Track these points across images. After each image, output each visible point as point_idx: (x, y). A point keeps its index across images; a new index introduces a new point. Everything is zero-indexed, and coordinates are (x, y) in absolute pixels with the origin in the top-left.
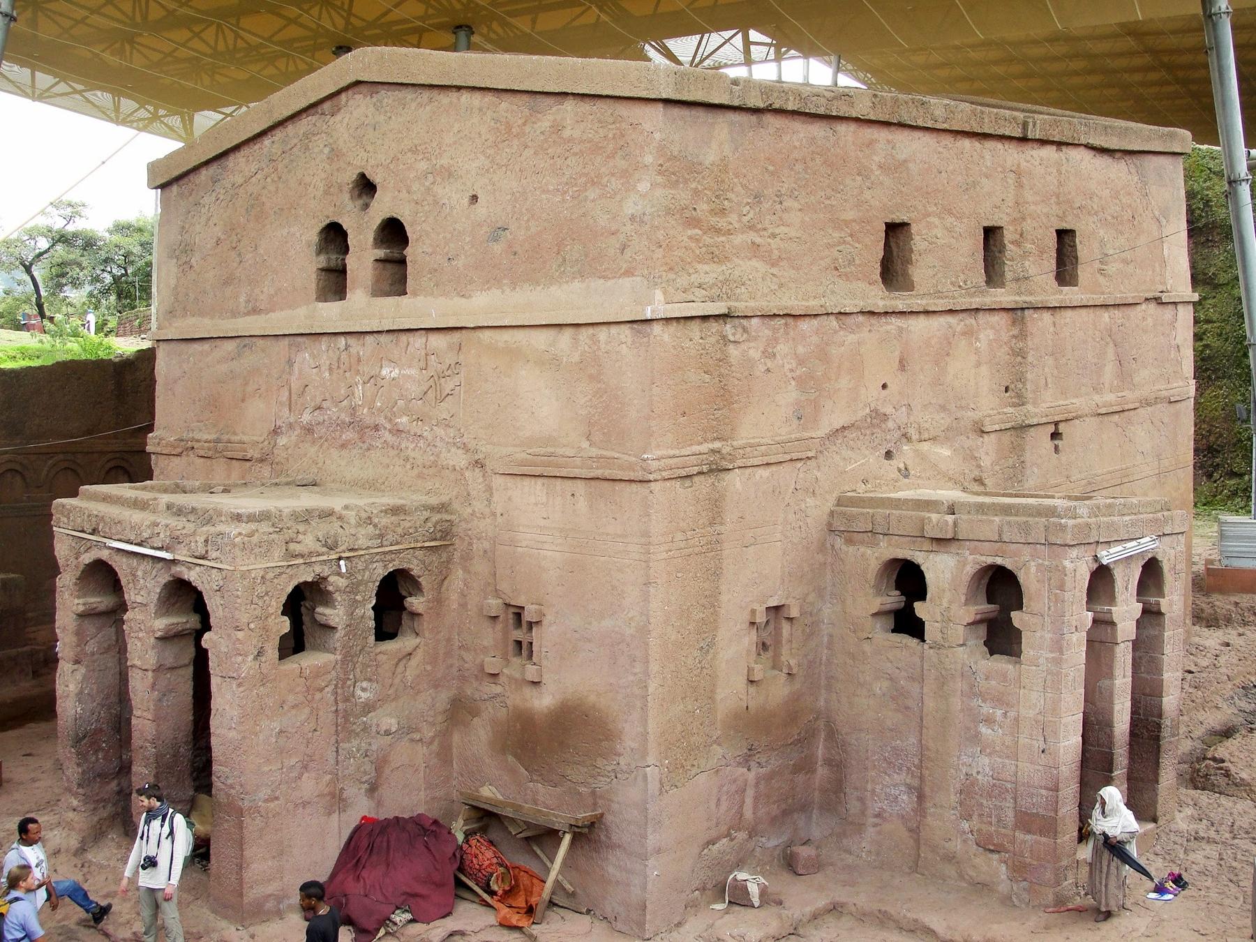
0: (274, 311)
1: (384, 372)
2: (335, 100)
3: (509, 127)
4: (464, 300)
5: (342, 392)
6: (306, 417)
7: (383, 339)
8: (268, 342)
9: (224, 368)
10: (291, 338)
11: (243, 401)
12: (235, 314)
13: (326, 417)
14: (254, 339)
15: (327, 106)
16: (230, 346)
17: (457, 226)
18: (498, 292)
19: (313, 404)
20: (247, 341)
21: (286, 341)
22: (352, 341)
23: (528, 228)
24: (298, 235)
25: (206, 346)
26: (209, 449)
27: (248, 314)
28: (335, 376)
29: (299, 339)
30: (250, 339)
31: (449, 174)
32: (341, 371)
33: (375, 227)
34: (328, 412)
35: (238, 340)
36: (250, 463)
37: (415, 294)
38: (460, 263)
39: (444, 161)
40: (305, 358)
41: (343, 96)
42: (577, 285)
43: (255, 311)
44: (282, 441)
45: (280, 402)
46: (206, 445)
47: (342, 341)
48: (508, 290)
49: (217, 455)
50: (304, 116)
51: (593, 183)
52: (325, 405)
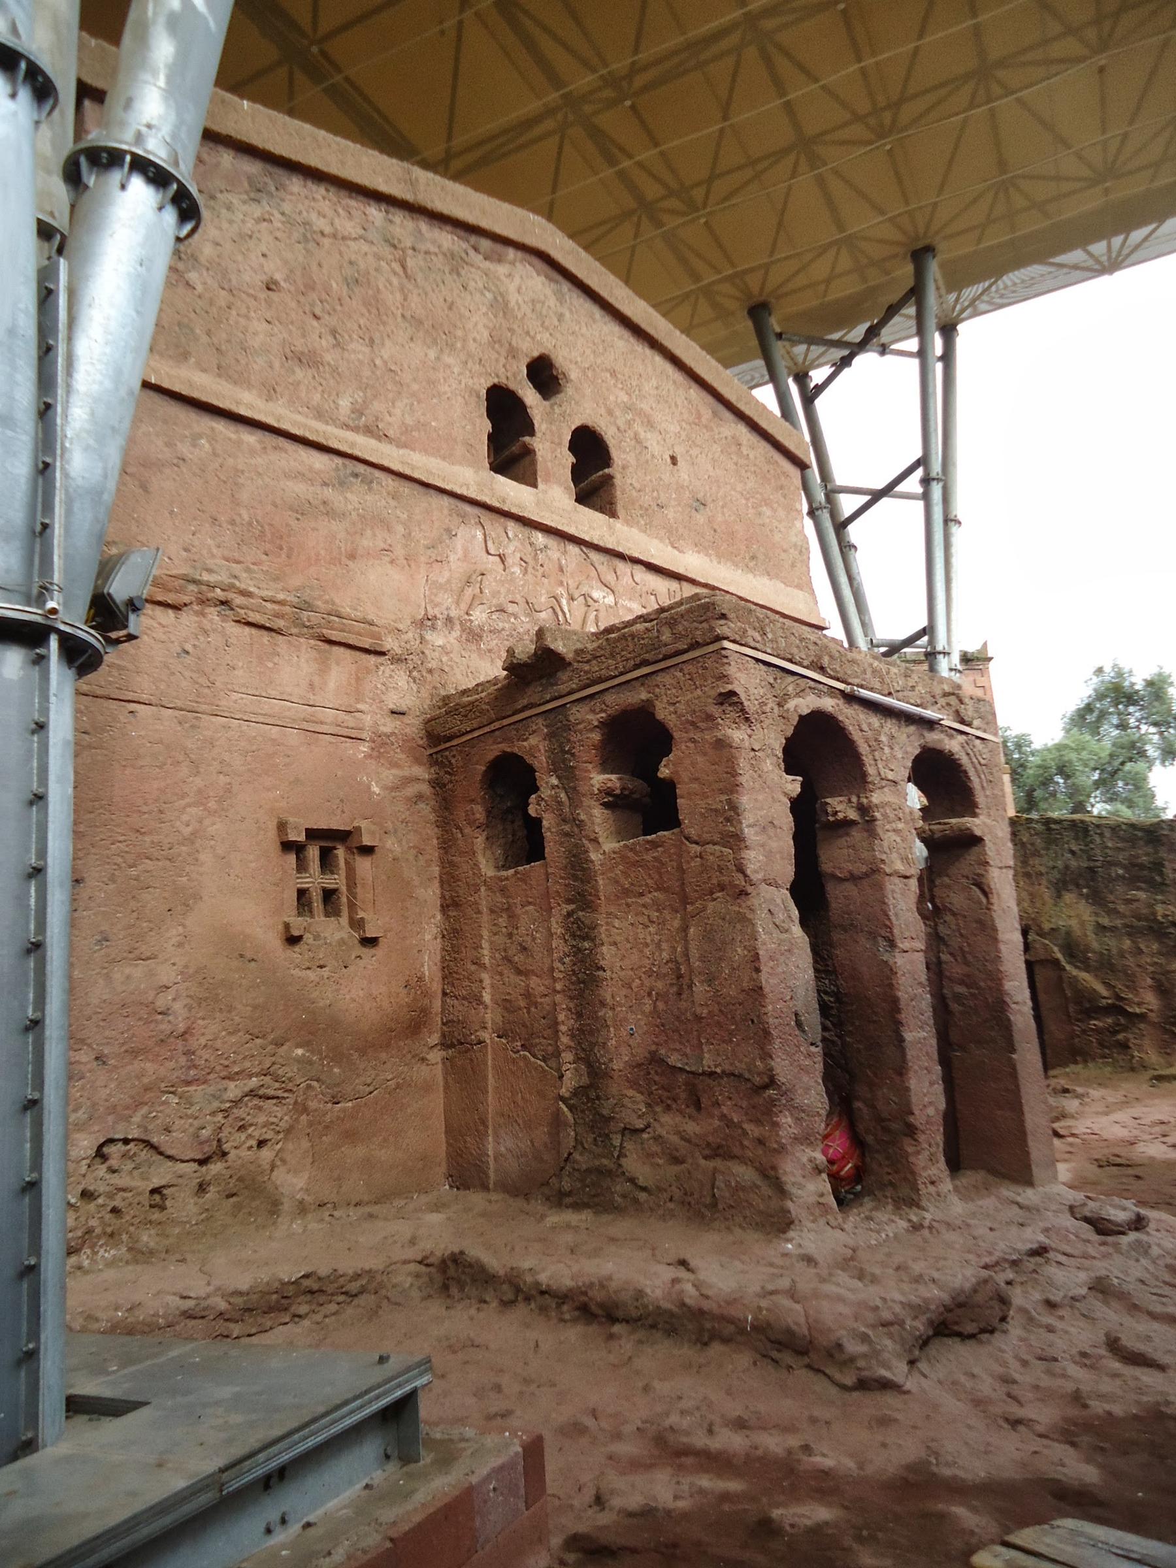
0: (413, 450)
1: (596, 594)
2: (499, 248)
3: (699, 416)
4: (677, 552)
5: (543, 599)
6: (479, 616)
7: (595, 556)
8: (406, 488)
9: (299, 489)
10: (452, 501)
11: (352, 556)
12: (320, 415)
13: (507, 626)
14: (377, 473)
15: (485, 244)
16: (320, 461)
17: (663, 477)
18: (707, 559)
19: (494, 602)
20: (361, 468)
21: (446, 501)
22: (552, 542)
23: (723, 514)
24: (456, 370)
25: (250, 438)
26: (278, 615)
27: (355, 429)
28: (529, 577)
29: (468, 509)
30: (369, 469)
31: (650, 424)
32: (539, 574)
33: (573, 428)
34: (512, 620)
35: (339, 461)
36: (381, 659)
37: (627, 523)
38: (671, 513)
39: (644, 406)
40: (474, 537)
41: (511, 253)
42: (765, 580)
43: (369, 431)
44: (437, 639)
45: (434, 582)
46: (268, 605)
47: (540, 538)
48: (715, 562)
49: (294, 631)
50: (449, 228)
51: (766, 505)
52: (511, 608)
